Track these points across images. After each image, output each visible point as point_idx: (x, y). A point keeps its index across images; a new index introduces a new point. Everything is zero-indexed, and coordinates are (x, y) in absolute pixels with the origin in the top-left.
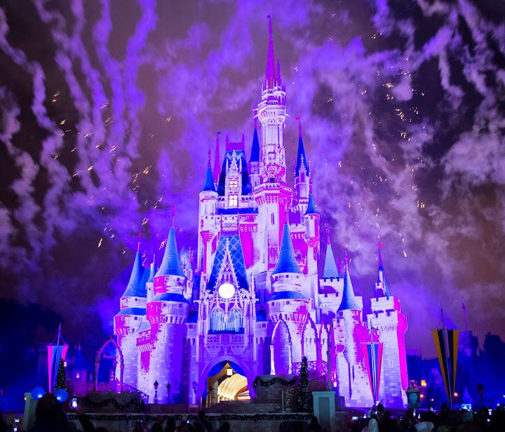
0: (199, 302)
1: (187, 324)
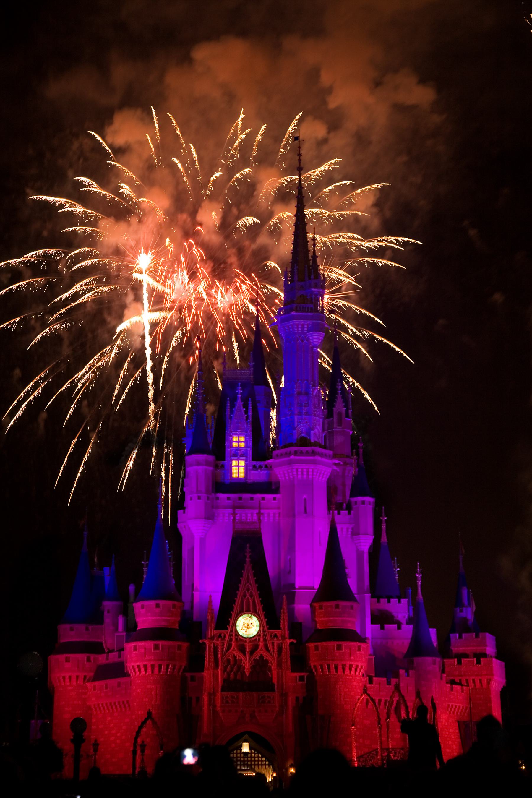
0: (207, 642)
1: (188, 675)
